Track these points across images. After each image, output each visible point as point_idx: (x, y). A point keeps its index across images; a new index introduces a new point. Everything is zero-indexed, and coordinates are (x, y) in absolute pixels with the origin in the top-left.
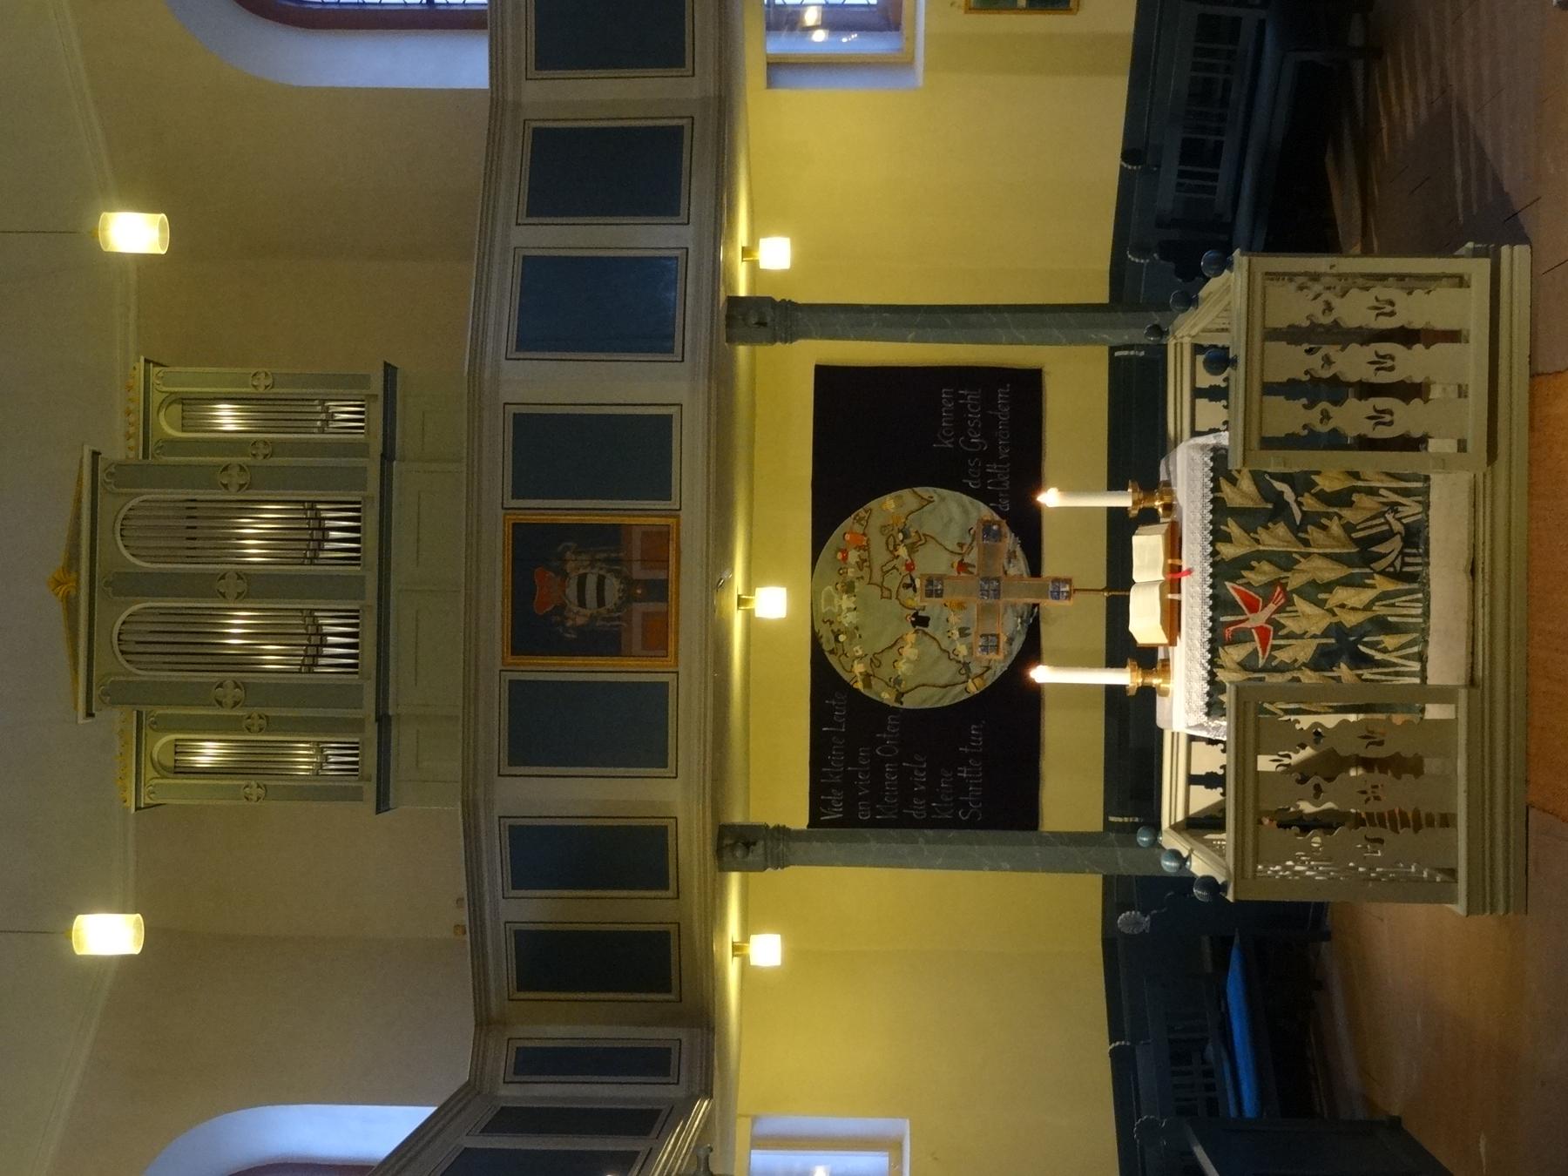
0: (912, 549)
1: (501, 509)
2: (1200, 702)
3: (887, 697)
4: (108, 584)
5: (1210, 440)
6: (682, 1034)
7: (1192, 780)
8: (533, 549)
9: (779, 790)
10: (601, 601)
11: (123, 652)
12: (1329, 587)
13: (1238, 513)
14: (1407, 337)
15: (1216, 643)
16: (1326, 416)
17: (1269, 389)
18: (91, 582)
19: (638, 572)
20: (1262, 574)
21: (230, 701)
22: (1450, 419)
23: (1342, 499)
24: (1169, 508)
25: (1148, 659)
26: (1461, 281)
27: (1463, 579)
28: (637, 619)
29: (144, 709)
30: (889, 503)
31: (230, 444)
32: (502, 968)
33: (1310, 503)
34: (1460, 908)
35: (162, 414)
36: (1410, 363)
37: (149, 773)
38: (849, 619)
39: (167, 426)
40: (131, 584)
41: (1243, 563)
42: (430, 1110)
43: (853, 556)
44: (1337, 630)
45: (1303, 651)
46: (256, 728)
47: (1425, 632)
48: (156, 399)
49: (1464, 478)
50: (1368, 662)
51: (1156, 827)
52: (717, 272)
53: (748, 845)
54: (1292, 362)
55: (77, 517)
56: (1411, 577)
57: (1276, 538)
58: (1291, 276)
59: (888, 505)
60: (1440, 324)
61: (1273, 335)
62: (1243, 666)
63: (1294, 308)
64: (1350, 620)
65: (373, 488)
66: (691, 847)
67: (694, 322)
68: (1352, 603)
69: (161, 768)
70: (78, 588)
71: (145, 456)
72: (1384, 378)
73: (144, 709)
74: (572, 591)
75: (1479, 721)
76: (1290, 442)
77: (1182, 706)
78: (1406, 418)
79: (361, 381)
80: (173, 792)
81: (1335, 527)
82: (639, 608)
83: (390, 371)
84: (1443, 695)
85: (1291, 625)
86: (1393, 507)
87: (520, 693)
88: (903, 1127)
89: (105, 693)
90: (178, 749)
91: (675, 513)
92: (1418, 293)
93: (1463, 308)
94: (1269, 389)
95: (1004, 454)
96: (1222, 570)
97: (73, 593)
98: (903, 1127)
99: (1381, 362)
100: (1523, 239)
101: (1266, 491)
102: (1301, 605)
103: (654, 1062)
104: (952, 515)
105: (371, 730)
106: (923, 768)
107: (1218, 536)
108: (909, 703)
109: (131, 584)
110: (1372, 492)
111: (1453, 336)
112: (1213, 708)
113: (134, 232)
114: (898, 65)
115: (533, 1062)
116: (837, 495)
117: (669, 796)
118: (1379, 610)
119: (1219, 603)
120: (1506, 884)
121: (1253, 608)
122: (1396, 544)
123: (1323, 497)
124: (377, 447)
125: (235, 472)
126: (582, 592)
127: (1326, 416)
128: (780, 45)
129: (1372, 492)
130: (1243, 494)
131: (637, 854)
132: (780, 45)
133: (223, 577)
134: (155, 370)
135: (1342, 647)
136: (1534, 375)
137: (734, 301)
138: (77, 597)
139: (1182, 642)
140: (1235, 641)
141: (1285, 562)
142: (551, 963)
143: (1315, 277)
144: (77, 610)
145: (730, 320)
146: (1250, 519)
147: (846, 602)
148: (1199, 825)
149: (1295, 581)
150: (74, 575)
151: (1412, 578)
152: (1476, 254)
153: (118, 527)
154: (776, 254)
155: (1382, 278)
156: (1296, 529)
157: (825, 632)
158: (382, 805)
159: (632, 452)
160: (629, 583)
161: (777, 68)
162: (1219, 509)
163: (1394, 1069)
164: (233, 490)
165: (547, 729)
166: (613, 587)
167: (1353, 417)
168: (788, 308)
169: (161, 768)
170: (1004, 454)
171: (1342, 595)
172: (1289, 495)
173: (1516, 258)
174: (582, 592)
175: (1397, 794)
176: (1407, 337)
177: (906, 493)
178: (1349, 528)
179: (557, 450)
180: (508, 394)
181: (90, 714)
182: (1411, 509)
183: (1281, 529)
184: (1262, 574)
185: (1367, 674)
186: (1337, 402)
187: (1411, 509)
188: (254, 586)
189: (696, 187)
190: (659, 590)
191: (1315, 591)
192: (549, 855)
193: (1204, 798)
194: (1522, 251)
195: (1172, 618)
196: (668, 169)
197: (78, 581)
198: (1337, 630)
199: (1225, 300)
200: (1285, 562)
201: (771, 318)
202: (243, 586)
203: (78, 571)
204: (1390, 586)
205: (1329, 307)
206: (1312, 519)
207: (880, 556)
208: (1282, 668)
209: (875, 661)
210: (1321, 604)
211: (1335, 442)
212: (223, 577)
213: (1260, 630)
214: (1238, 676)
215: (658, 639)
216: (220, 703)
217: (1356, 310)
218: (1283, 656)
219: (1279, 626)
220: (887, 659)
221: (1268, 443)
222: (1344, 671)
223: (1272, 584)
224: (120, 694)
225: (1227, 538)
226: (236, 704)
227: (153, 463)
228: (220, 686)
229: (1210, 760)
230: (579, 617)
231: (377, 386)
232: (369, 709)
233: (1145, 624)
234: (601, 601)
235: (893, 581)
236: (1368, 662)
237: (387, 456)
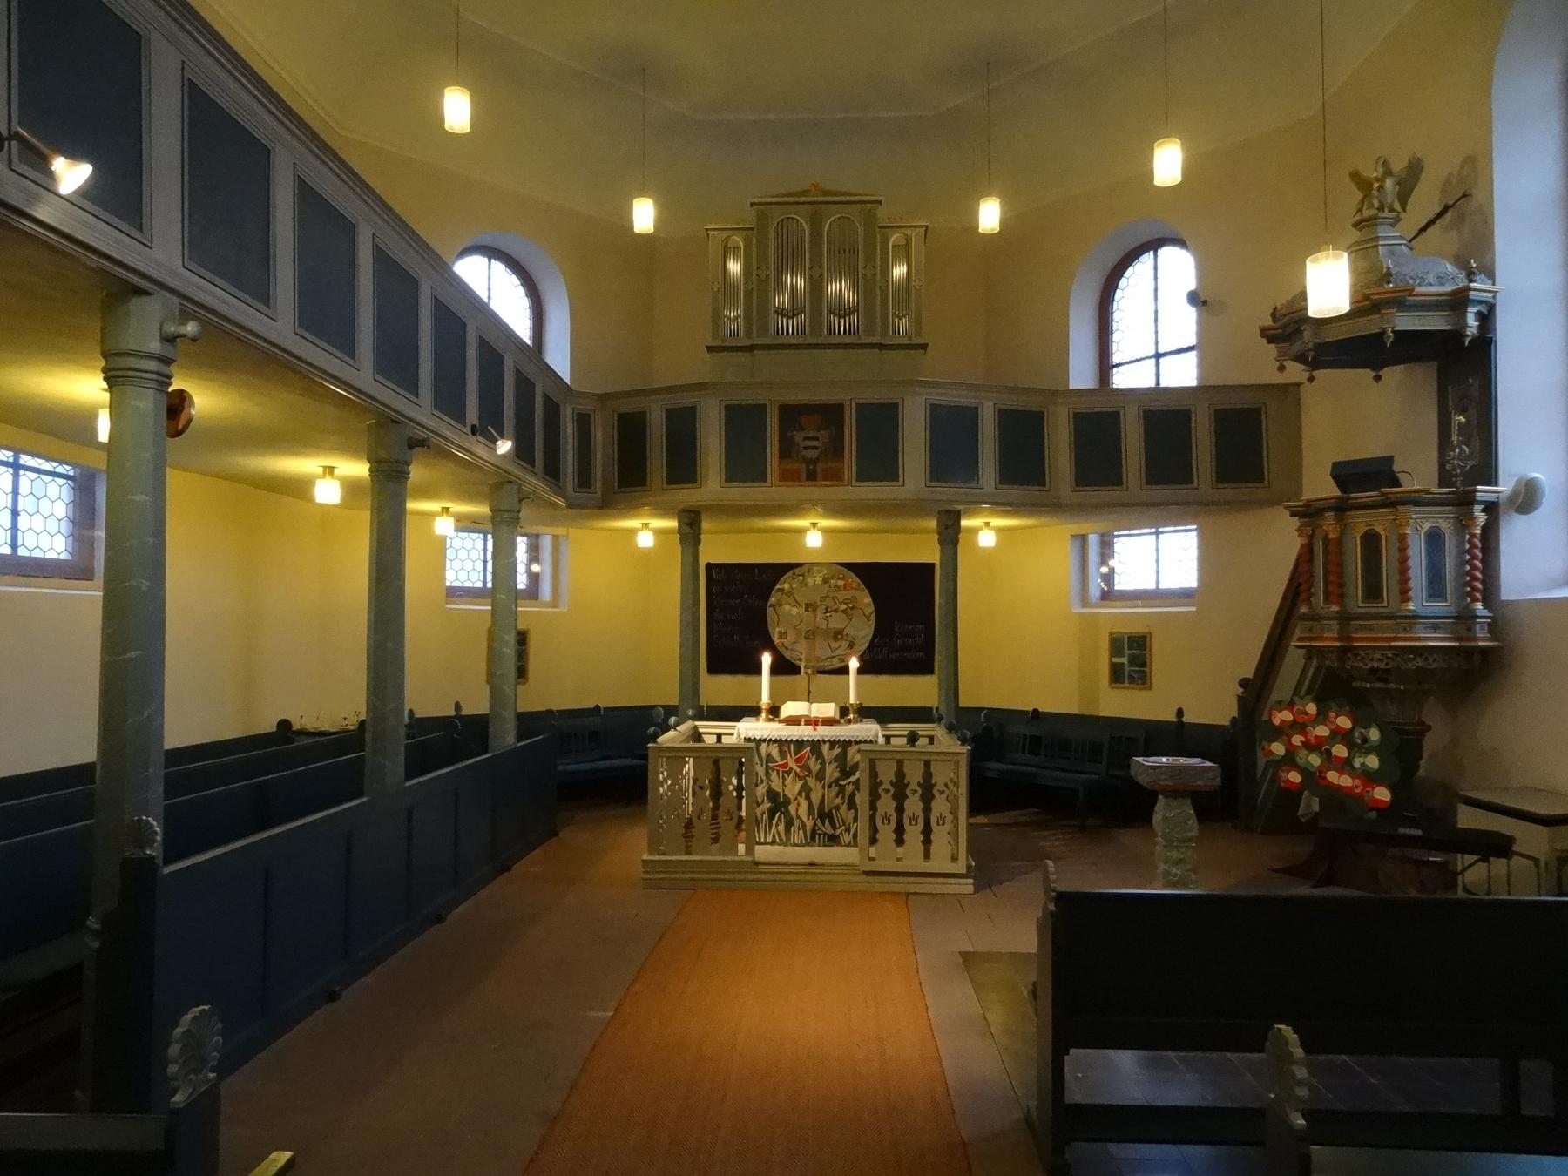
0: (844, 611)
1: (850, 399)
2: (751, 735)
3: (772, 600)
5: (881, 740)
6: (599, 494)
7: (719, 736)
8: (831, 415)
9: (721, 547)
10: (806, 448)
12: (808, 798)
13: (844, 754)
14: (927, 831)
15: (779, 742)
16: (887, 791)
17: (900, 763)
18: (816, 203)
19: (820, 466)
20: (814, 765)
22: (886, 855)
23: (852, 805)
24: (849, 721)
25: (774, 711)
26: (954, 859)
27: (807, 860)
28: (796, 466)
30: (868, 600)
31: (886, 272)
32: (630, 406)
33: (850, 789)
34: (645, 857)
36: (913, 834)
37: (724, 235)
38: (810, 581)
39: (894, 238)
40: (816, 222)
41: (820, 756)
42: (568, 381)
43: (841, 583)
44: (787, 802)
45: (776, 785)
47: (786, 845)
48: (908, 232)
49: (857, 861)
50: (772, 817)
51: (694, 718)
52: (974, 505)
53: (690, 525)
54: (914, 776)
55: (845, 194)
56: (813, 838)
57: (832, 772)
58: (957, 774)
59: (866, 599)
60: (933, 848)
61: (927, 764)
62: (769, 756)
63: (940, 776)
64: (792, 808)
66: (688, 496)
67: (947, 492)
68: (800, 809)
69: (726, 241)
72: (906, 821)
74: (811, 434)
75: (739, 866)
76: (874, 774)
77: (748, 728)
78: (887, 832)
79: (918, 334)
80: (715, 248)
81: (838, 801)
82: (803, 467)
83: (924, 347)
84: (750, 851)
85: (789, 780)
86: (848, 830)
87: (761, 409)
88: (563, 608)
91: (850, 484)
92: (949, 838)
93: (941, 860)
94: (900, 763)
95: (892, 656)
96: (816, 745)
98: (563, 608)
99: (914, 819)
100: (977, 889)
101: (855, 768)
102: (799, 785)
103: (584, 480)
104: (864, 630)
106: (737, 616)
107: (833, 744)
108: (770, 610)
109: (816, 222)
110: (855, 819)
111: (927, 856)
112: (748, 740)
113: (989, 216)
114: (1084, 600)
115: (583, 422)
116: (872, 575)
117: (712, 485)
118: (797, 822)
119: (800, 744)
120: (658, 879)
121: (797, 761)
122: (829, 830)
123: (852, 796)
124: (887, 342)
126: (810, 439)
127: (887, 791)
128: (1093, 539)
129: (855, 819)
130: (853, 755)
131: (683, 469)
132: (1093, 539)
134: (922, 230)
135: (778, 804)
136: (908, 894)
137: (957, 516)
139: (782, 726)
140: (781, 752)
141: (820, 776)
142: (631, 429)
143: (956, 784)
145: (949, 512)
146: (841, 759)
147: (819, 580)
148: (697, 736)
149: (811, 781)
151: (813, 838)
152: (969, 867)
154: (987, 539)
155: (956, 818)
156: (836, 782)
157: (805, 569)
158: (710, 349)
159: (880, 461)
160: (816, 461)
161: (1082, 539)
162: (846, 744)
163: (576, 836)
165: (743, 424)
166: (812, 454)
167: (887, 804)
168: (955, 542)
169: (726, 241)
170: (892, 656)
171: (804, 804)
172: (853, 779)
173: (967, 886)
174: (810, 439)
175: (703, 827)
176: (927, 831)
177: (872, 608)
178: (837, 808)
179: (881, 426)
180: (908, 400)
181: (752, 204)
182: (846, 838)
183: (836, 774)
184: (814, 765)
185: (766, 816)
186: (894, 797)
187: (846, 838)
188: (816, 286)
189: (1015, 493)
190: (812, 477)
191: (806, 791)
192: (683, 427)
193: (710, 740)
194: (971, 889)
195: (793, 721)
196: (1023, 475)
198: (787, 802)
199: (946, 743)
200: (820, 776)
201: (950, 534)
202: (816, 277)
204: (809, 829)
205: (942, 792)
206: (843, 788)
207: (842, 595)
208: (767, 773)
209: (790, 594)
210: (800, 794)
211: (874, 797)
213: (785, 766)
214: (764, 754)
215: (788, 476)
217: (940, 806)
218: (774, 775)
219: (788, 773)
220: (791, 600)
221: (872, 764)
222: (767, 805)
223: (810, 771)
224: (762, 219)
225: (832, 748)
227: (876, 231)
229: (726, 740)
230: (798, 437)
233: (790, 709)
234: (806, 448)
235: (829, 602)
236: (772, 817)
237: (881, 347)
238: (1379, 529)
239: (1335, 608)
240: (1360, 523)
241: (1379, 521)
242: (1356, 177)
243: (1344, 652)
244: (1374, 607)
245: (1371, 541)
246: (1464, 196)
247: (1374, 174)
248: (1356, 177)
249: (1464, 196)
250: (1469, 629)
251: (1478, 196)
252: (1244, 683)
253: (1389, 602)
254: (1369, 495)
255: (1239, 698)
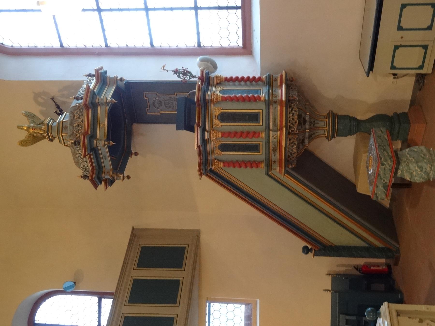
238: (217, 113)
239: (263, 135)
240: (213, 122)
241: (214, 112)
242: (23, 143)
243: (288, 133)
244: (263, 118)
245: (225, 117)
246: (53, 99)
247: (23, 135)
248: (23, 143)
249: (53, 99)
250: (275, 80)
251: (54, 92)
252: (306, 250)
253: (259, 108)
254: (198, 113)
255: (314, 255)
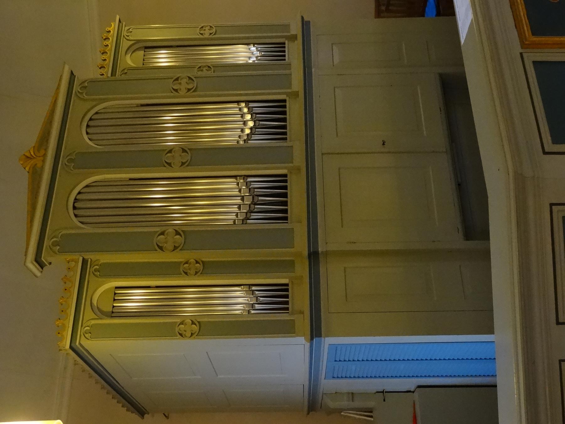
4: (70, 161)
11: (76, 216)
21: (170, 246)
29: (90, 256)
35: (128, 56)
37: (87, 315)
46: (193, 272)
48: (125, 44)
65: (297, 84)
70: (44, 161)
71: (113, 73)
73: (88, 256)
89: (55, 244)
90: (116, 294)
97: (39, 165)
105: (302, 269)
125: (184, 81)
133: (170, 151)
138: (42, 168)
144: (41, 176)
150: (42, 152)
153: (85, 124)
164: (183, 92)
197: (45, 155)
202: (187, 157)
203: (46, 150)
212: (170, 151)
216: (161, 248)
226: (175, 248)
227: (117, 78)
228: (162, 233)
231: (296, 29)
232: (301, 244)
